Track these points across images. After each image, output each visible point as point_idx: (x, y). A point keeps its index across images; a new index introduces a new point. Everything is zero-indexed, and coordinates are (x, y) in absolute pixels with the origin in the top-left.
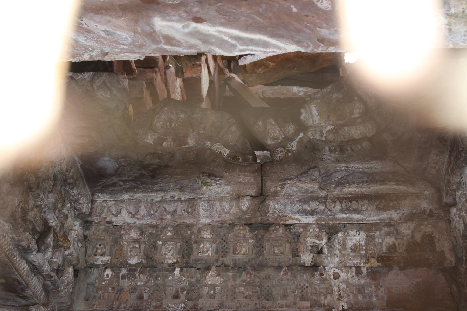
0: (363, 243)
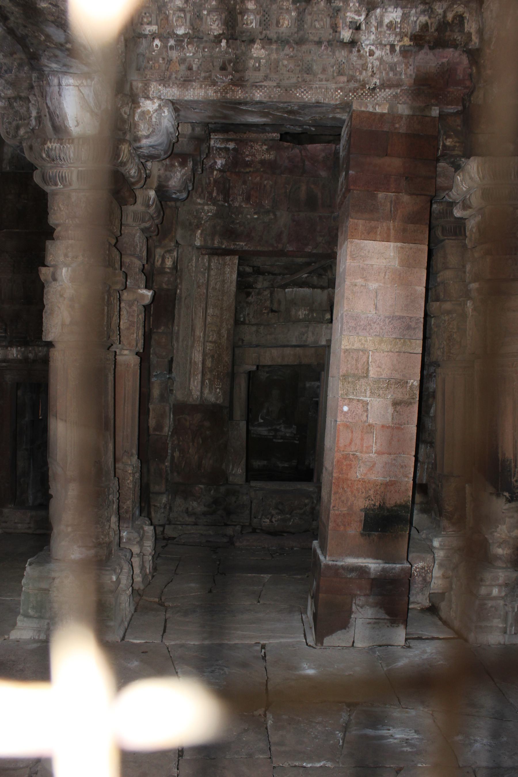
0: (399, 20)
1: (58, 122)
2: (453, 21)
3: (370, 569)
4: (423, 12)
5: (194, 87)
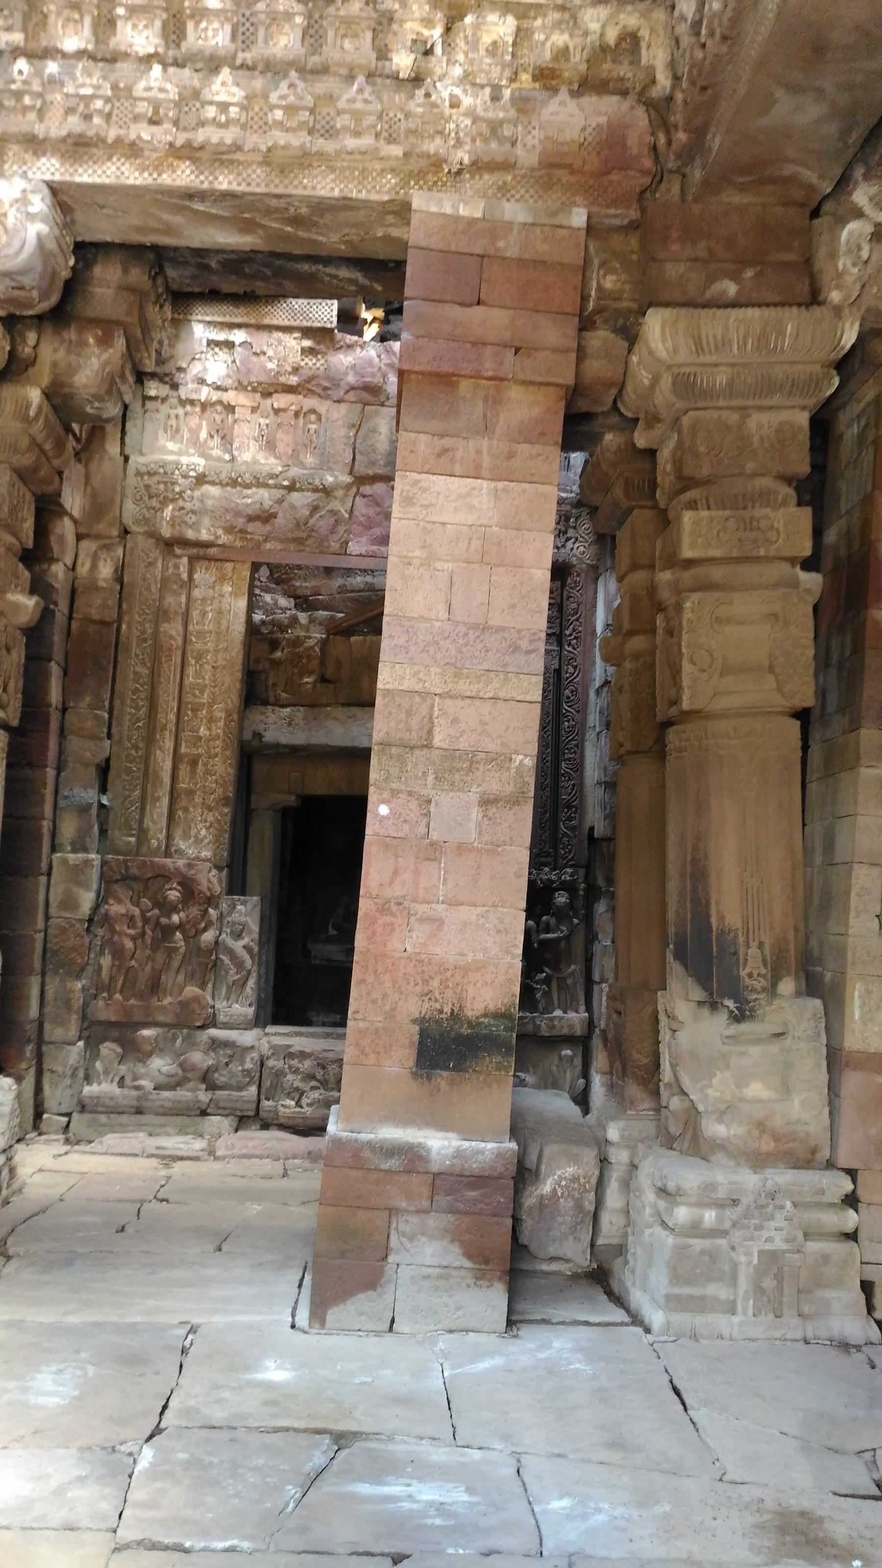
0: (510, 40)
2: (617, 45)
3: (429, 1151)
4: (558, 25)
5: (95, 158)
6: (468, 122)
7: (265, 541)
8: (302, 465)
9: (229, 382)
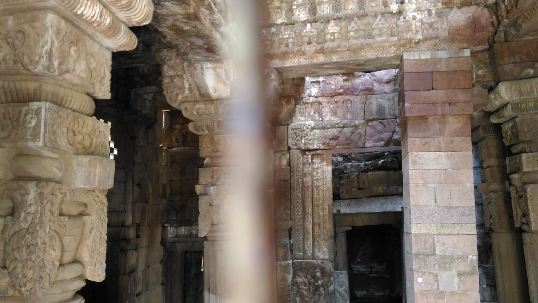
1: (203, 91)
6: (420, 24)
7: (336, 146)
8: (346, 119)
9: (319, 95)
